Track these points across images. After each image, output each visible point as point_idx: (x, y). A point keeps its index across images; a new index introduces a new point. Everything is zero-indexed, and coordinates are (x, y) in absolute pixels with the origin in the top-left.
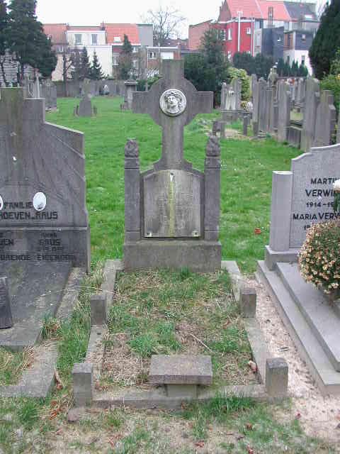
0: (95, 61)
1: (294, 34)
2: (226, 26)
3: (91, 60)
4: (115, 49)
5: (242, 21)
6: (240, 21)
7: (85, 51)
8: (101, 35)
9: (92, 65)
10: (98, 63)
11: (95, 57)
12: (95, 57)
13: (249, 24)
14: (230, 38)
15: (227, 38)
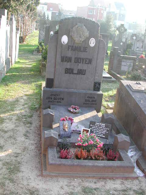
0: (48, 17)
1: (118, 14)
2: (93, 9)
3: (46, 17)
4: (53, 13)
5: (100, 8)
6: (99, 7)
7: (44, 14)
8: (46, 7)
9: (47, 19)
10: (49, 18)
11: (48, 16)
12: (48, 16)
13: (102, 9)
14: (94, 14)
15: (93, 13)
